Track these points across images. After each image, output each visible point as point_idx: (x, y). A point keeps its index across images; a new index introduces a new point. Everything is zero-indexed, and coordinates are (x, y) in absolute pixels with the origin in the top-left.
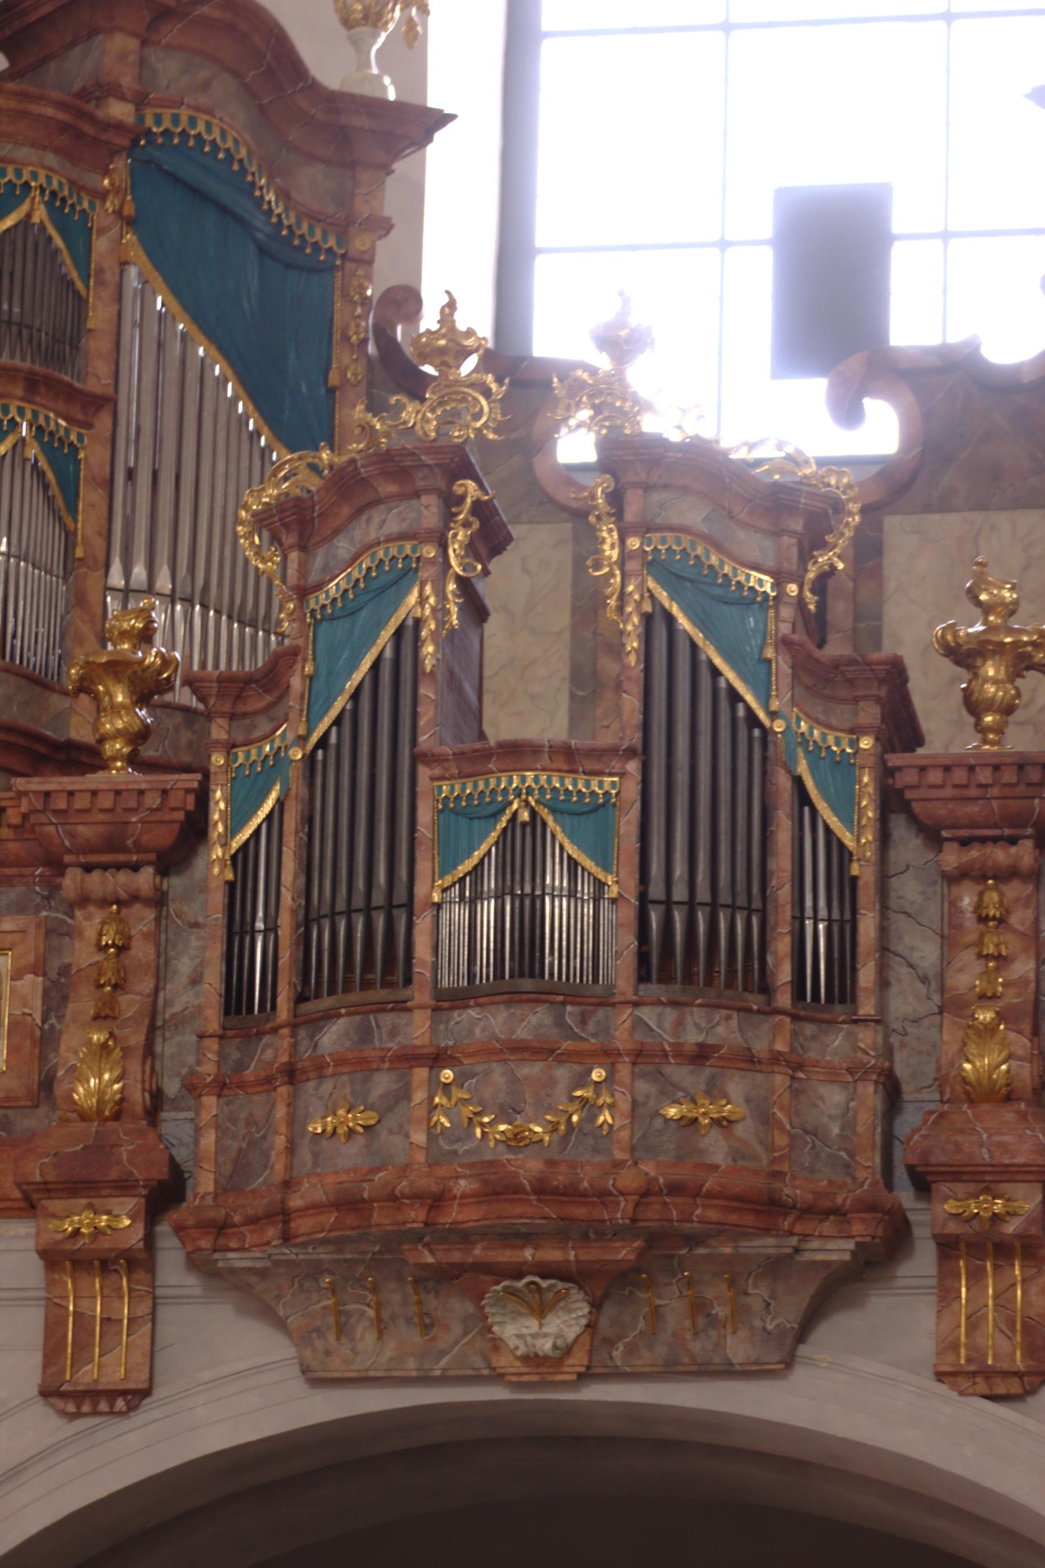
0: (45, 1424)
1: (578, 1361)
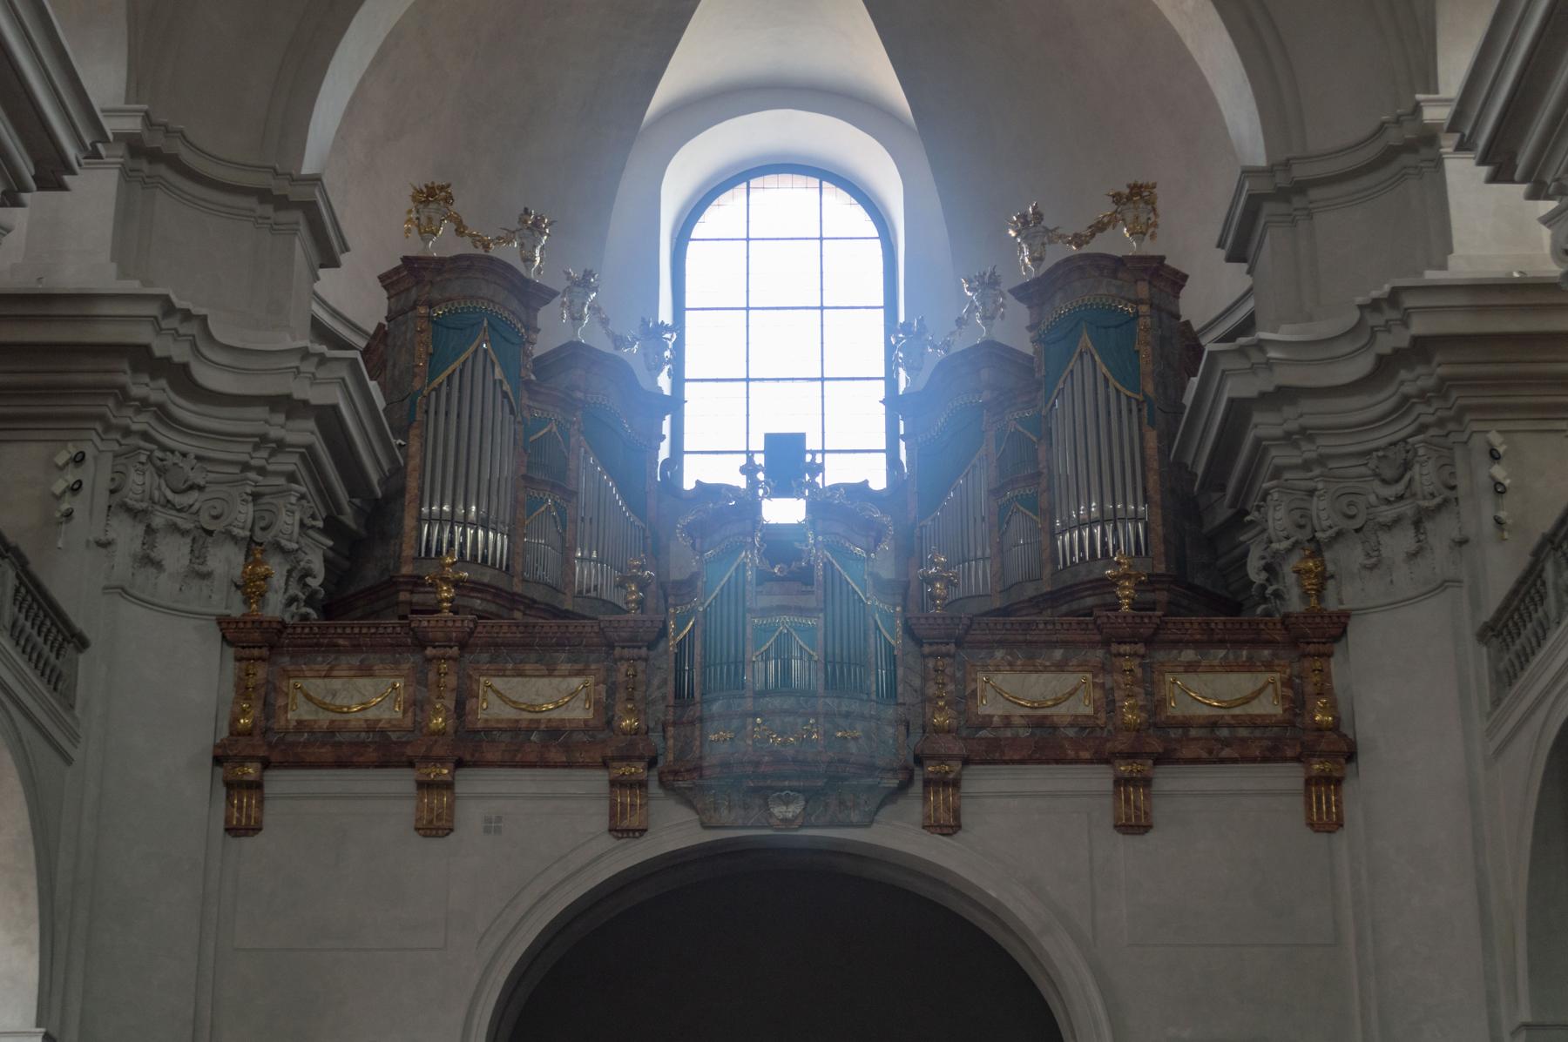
0: (608, 842)
1: (799, 821)
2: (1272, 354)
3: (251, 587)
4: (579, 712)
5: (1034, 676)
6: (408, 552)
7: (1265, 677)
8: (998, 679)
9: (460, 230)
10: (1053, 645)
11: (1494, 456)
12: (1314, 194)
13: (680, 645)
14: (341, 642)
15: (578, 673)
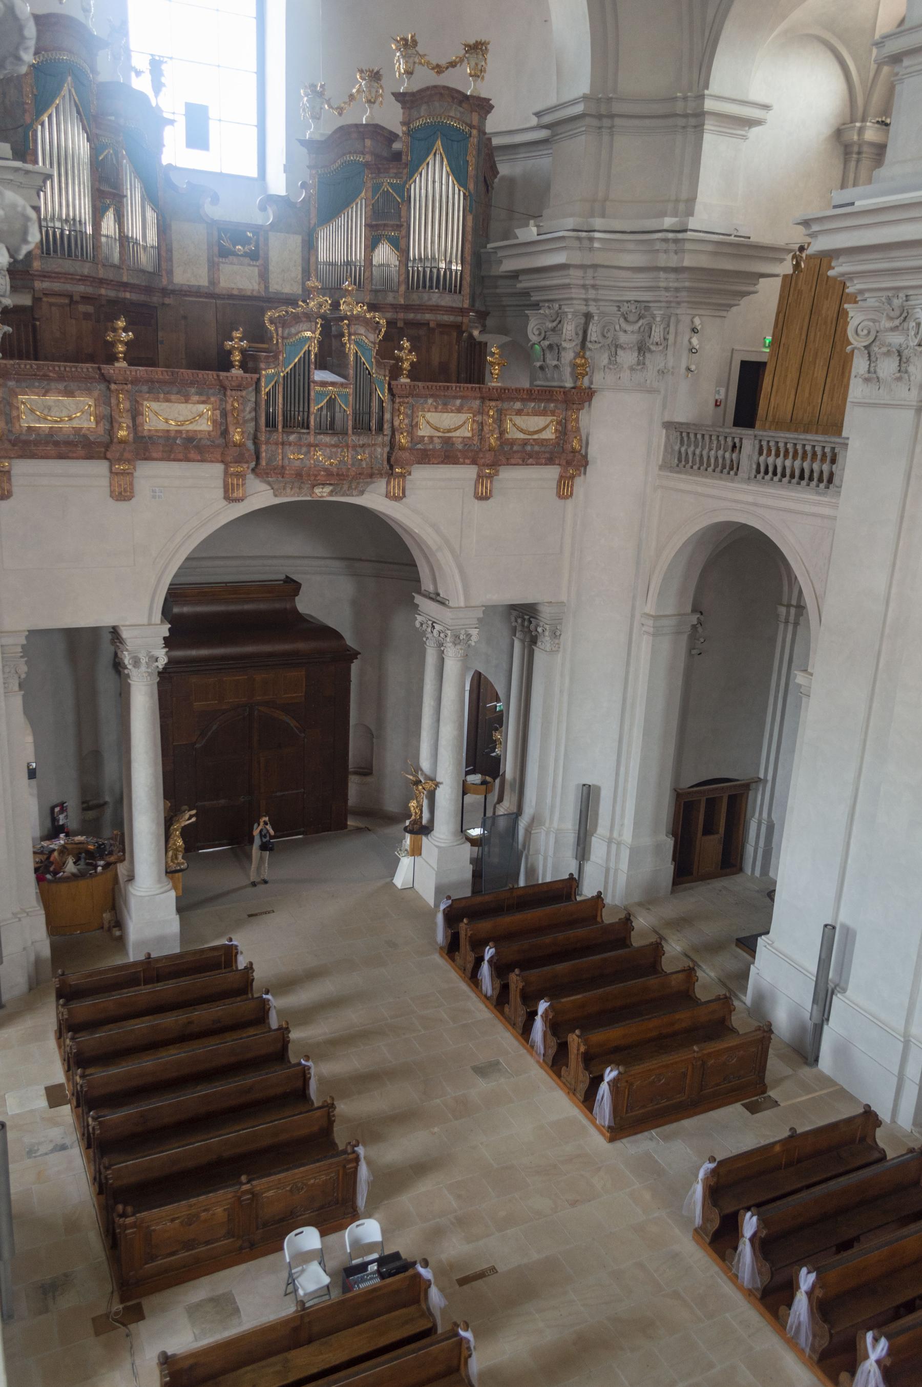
2: (596, 245)
4: (204, 426)
5: (446, 414)
7: (550, 418)
8: (429, 415)
10: (455, 397)
11: (694, 330)
12: (617, 121)
13: (268, 394)
14: (51, 374)
15: (203, 402)
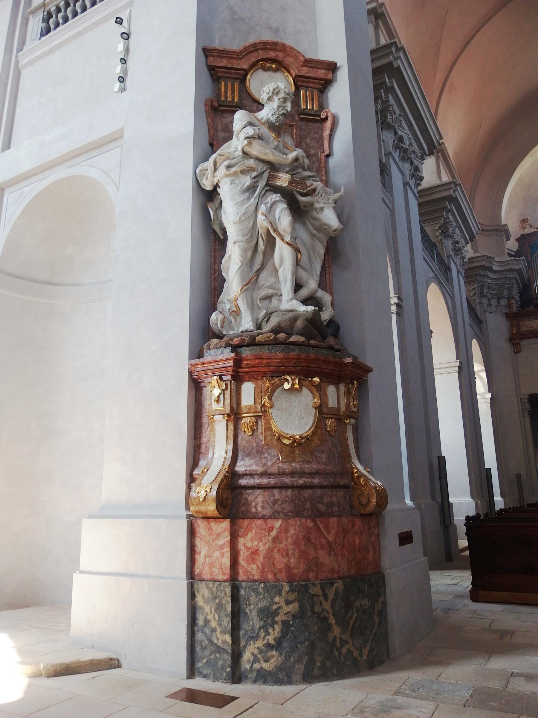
3: (509, 306)
6: (534, 293)
9: (531, 226)
